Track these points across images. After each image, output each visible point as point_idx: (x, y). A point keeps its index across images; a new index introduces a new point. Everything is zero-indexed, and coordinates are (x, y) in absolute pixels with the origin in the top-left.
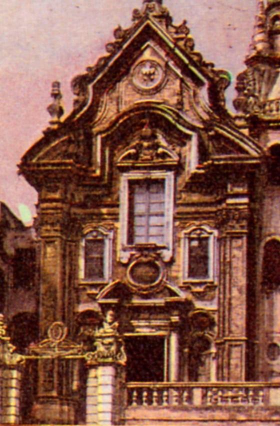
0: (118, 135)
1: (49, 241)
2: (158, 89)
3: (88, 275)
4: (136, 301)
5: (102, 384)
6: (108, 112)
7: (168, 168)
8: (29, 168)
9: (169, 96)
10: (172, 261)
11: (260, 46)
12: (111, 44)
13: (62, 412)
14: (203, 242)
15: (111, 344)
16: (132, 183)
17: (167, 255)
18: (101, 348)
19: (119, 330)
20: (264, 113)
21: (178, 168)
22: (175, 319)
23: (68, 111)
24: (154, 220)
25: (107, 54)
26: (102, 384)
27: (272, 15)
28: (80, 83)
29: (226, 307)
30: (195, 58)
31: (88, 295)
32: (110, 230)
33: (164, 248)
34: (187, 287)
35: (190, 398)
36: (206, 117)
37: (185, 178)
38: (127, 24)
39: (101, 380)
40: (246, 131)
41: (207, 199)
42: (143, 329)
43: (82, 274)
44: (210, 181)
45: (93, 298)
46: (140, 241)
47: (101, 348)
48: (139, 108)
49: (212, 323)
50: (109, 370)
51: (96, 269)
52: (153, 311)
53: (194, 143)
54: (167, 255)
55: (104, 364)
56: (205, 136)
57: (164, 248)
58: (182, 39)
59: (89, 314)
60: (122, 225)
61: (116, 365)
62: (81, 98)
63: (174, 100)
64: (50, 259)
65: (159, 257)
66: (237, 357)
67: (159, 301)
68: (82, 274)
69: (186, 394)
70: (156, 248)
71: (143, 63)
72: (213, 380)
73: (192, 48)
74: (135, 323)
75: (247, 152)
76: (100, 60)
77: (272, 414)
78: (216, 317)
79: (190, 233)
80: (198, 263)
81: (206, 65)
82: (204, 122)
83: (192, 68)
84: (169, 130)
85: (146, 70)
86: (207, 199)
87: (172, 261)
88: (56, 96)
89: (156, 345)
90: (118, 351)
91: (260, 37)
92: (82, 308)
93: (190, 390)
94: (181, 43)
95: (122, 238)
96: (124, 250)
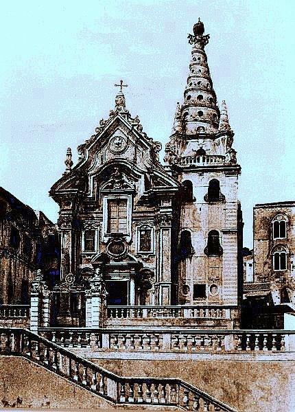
0: (103, 176)
1: (65, 232)
2: (123, 152)
3: (86, 249)
4: (112, 263)
5: (93, 308)
6: (98, 164)
7: (129, 193)
8: (54, 193)
9: (129, 155)
10: (131, 242)
11: (177, 129)
12: (98, 128)
13: (73, 321)
14: (148, 232)
15: (98, 285)
16: (109, 201)
17: (128, 239)
18: (93, 287)
19: (104, 278)
20: (180, 164)
21: (134, 193)
22: (133, 272)
23: (76, 162)
24: (121, 221)
25: (96, 134)
26: (93, 308)
27: (184, 112)
28: (82, 148)
29: (159, 266)
30: (143, 135)
31: (87, 259)
32: (98, 226)
33: (127, 235)
34: (139, 256)
35: (141, 314)
36: (149, 166)
37: (137, 198)
38: (107, 118)
39: (93, 304)
40: (170, 174)
41: (150, 209)
42: (116, 277)
43: (83, 249)
44: (152, 200)
45: (88, 261)
46: (112, 231)
47: (93, 287)
48: (114, 160)
49: (152, 274)
50: (98, 299)
51: (90, 247)
52: (122, 268)
53: (142, 180)
54: (128, 239)
55: (94, 296)
56: (148, 176)
57: (127, 235)
58: (136, 125)
59: (87, 269)
60: (104, 223)
61: (101, 297)
62: (82, 156)
63: (131, 158)
64: (66, 243)
65: (124, 240)
66: (166, 292)
67: (124, 263)
68: (83, 249)
69: (139, 311)
70: (122, 235)
71: (115, 138)
72: (153, 305)
73: (141, 130)
74: (111, 274)
75: (169, 184)
76: (93, 136)
77: (185, 323)
78: (155, 271)
79: (140, 228)
80: (145, 244)
81: (149, 139)
82: (148, 169)
83: (141, 140)
84: (129, 172)
85: (117, 141)
86: (150, 209)
87: (131, 242)
88: (70, 155)
89: (123, 287)
90: (102, 289)
91: (177, 124)
92: (82, 266)
93: (141, 309)
94: (135, 128)
95: (104, 231)
96: (105, 236)
